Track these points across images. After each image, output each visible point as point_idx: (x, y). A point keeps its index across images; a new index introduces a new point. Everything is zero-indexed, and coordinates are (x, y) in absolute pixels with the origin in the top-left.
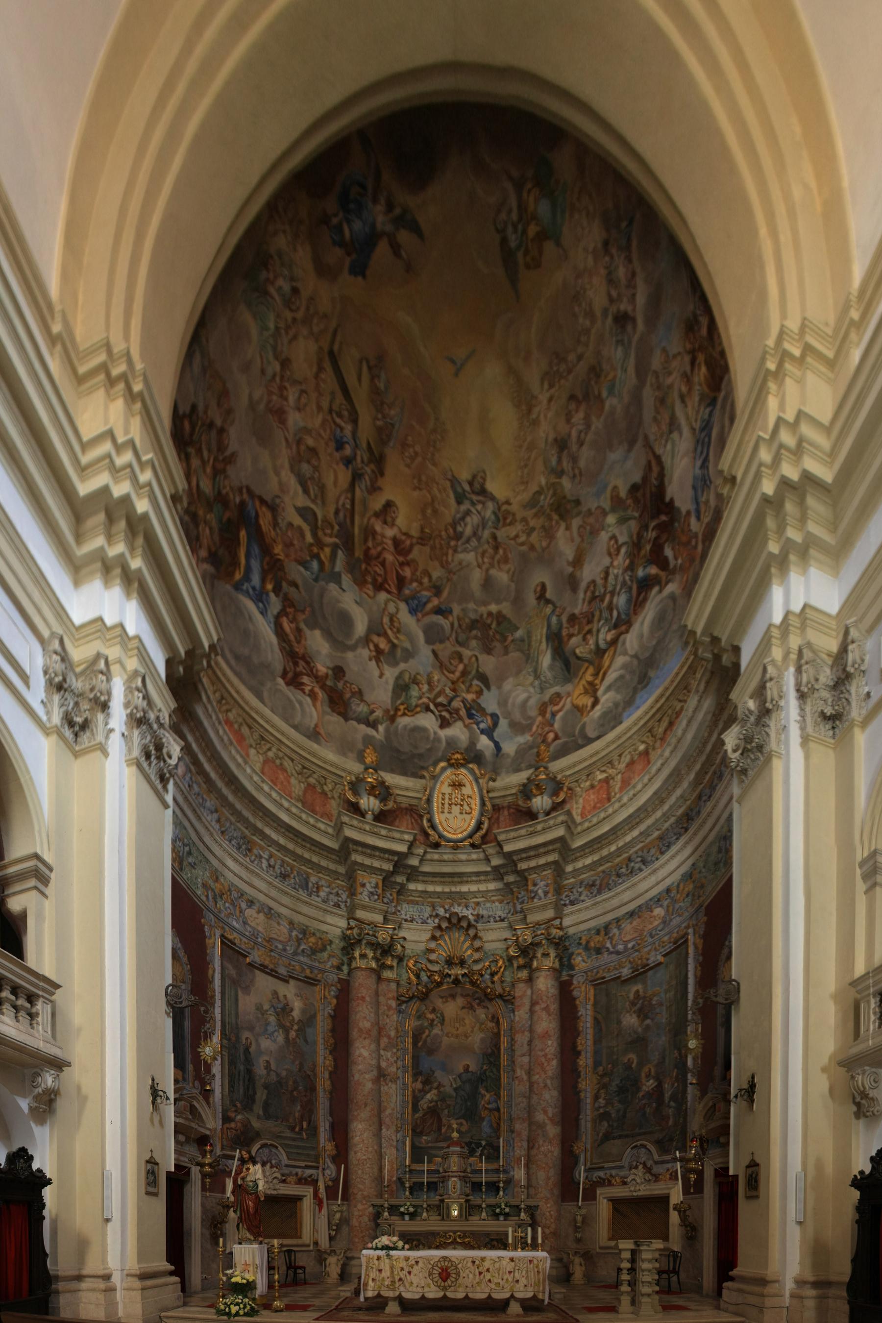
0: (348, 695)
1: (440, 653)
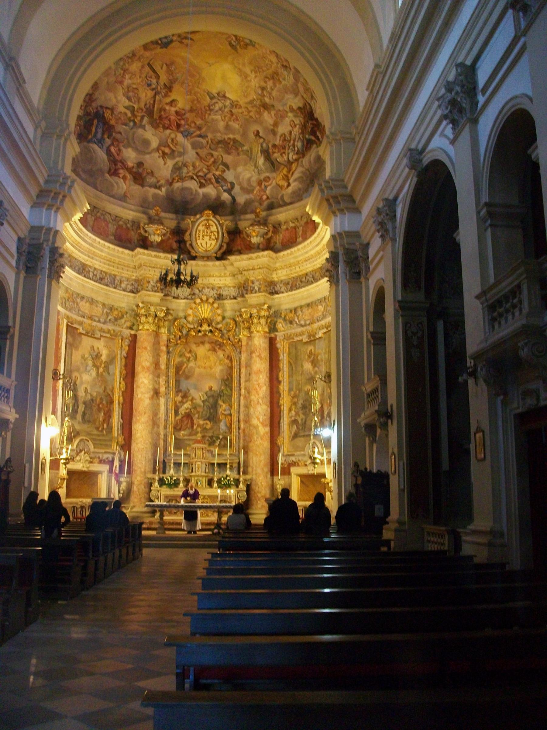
0: (145, 175)
1: (200, 154)
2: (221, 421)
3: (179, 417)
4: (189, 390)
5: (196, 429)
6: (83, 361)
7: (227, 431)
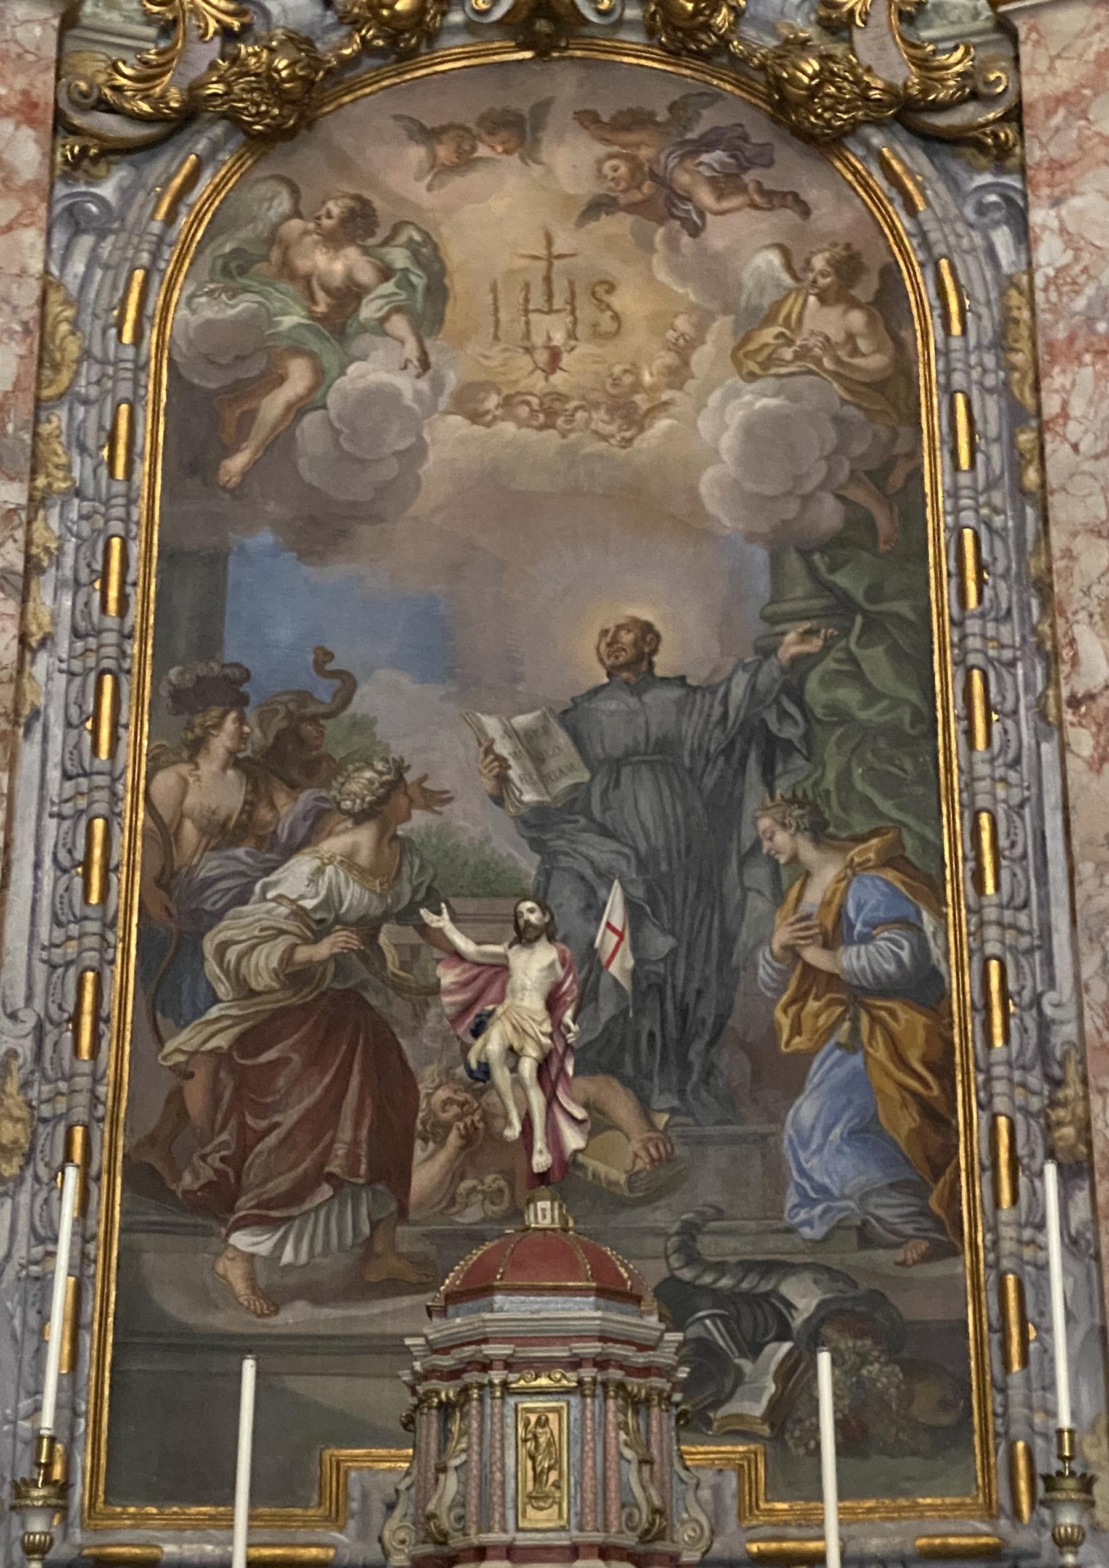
2: (787, 1076)
3: (208, 1033)
4: (347, 685)
5: (449, 1197)
7: (890, 1211)
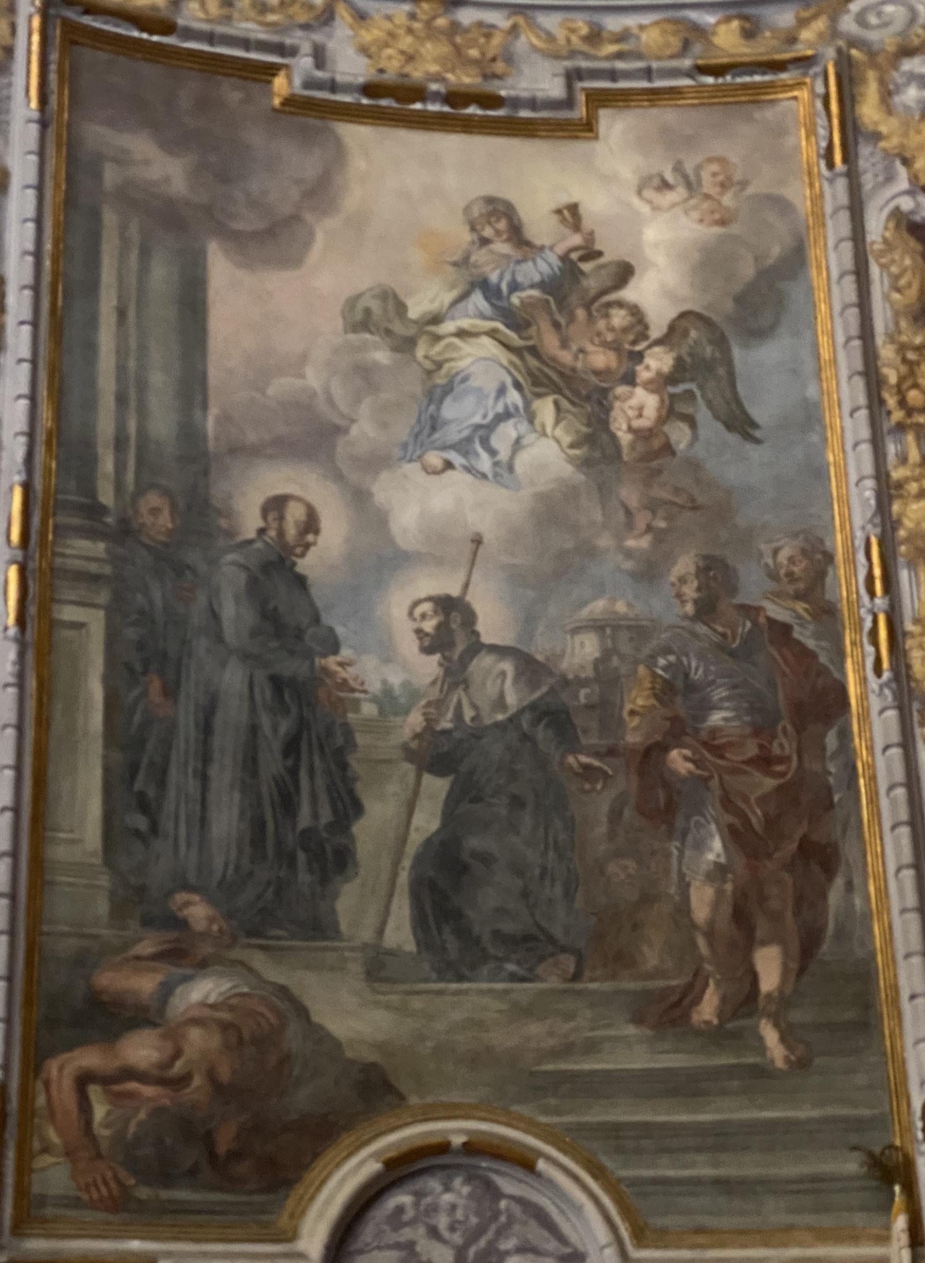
6: (382, 356)
